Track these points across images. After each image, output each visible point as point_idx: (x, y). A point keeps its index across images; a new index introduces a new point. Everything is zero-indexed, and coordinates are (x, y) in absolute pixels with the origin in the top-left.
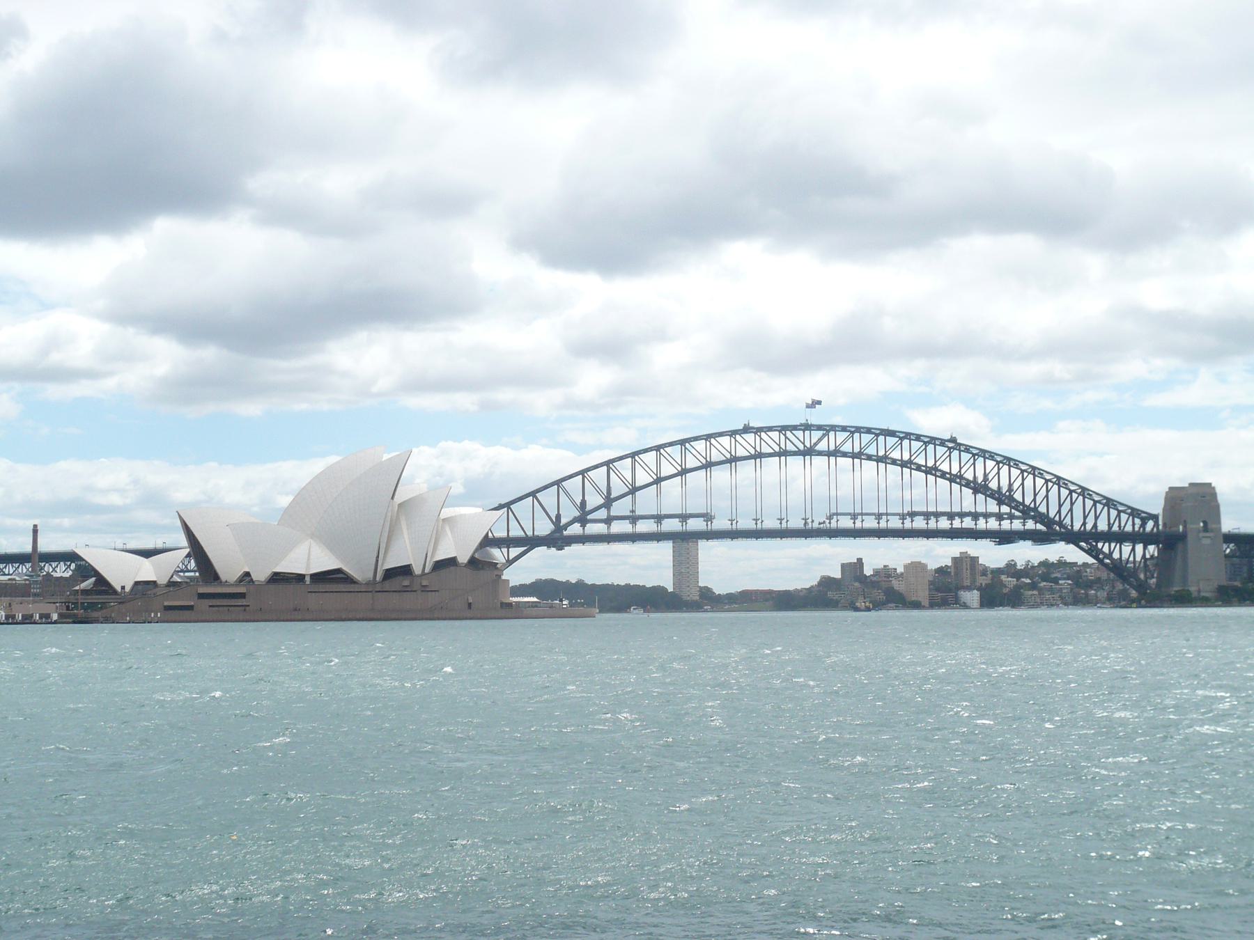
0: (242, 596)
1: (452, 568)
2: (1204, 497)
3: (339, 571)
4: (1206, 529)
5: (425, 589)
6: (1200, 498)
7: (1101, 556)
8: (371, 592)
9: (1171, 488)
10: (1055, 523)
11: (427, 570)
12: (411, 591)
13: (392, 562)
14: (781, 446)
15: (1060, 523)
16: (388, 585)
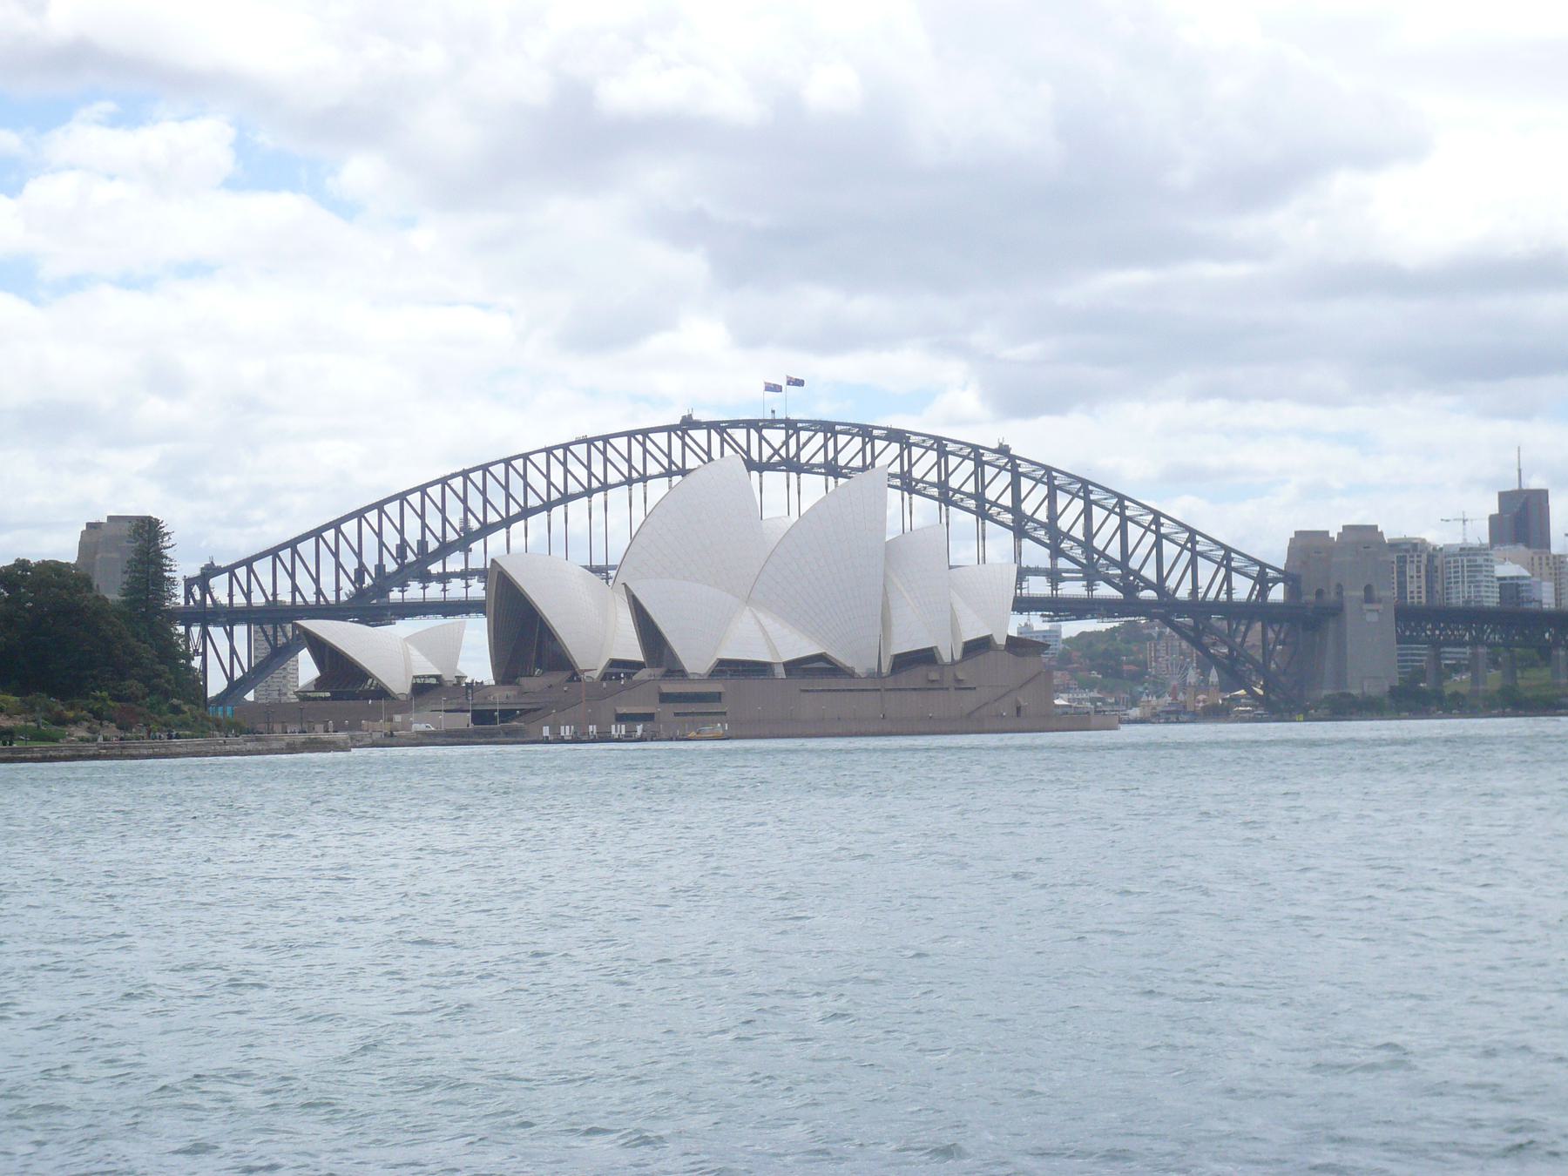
0: (716, 697)
1: (991, 653)
2: (1368, 547)
3: (821, 657)
4: (1369, 597)
5: (960, 686)
6: (1362, 549)
7: (1206, 640)
8: (879, 690)
9: (1296, 532)
10: (1148, 585)
11: (958, 656)
12: (942, 689)
13: (902, 645)
14: (802, 453)
15: (1159, 586)
16: (905, 679)
